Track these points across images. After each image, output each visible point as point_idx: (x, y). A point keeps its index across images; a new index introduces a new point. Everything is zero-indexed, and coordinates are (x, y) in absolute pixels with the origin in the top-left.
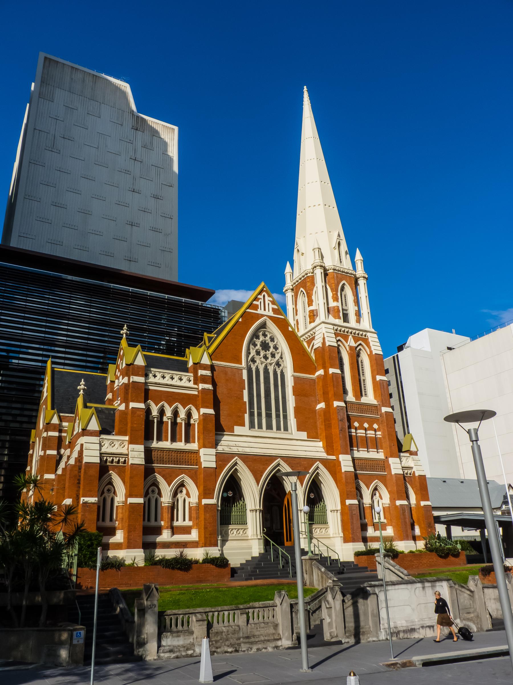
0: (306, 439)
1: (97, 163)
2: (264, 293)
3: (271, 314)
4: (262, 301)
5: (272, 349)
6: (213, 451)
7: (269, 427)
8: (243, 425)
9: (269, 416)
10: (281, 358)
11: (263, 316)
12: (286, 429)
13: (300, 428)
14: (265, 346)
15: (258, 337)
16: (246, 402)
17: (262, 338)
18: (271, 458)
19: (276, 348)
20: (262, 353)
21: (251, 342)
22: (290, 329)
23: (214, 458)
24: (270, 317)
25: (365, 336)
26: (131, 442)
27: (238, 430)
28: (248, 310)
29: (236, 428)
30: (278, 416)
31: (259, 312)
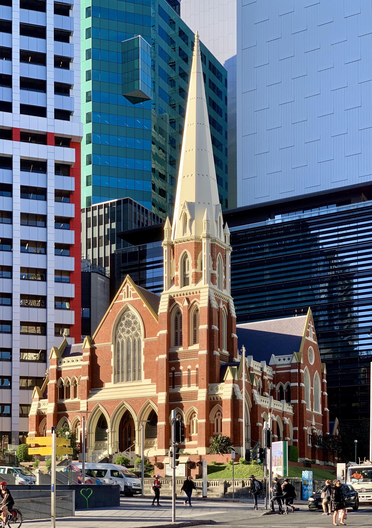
0: (151, 383)
3: (131, 299)
4: (126, 291)
6: (85, 401)
7: (128, 380)
9: (128, 372)
10: (140, 329)
11: (125, 302)
12: (139, 378)
13: (146, 378)
14: (128, 324)
16: (112, 366)
18: (118, 401)
19: (136, 323)
20: (127, 329)
21: (118, 324)
25: (200, 292)
28: (116, 302)
30: (134, 371)
31: (124, 300)
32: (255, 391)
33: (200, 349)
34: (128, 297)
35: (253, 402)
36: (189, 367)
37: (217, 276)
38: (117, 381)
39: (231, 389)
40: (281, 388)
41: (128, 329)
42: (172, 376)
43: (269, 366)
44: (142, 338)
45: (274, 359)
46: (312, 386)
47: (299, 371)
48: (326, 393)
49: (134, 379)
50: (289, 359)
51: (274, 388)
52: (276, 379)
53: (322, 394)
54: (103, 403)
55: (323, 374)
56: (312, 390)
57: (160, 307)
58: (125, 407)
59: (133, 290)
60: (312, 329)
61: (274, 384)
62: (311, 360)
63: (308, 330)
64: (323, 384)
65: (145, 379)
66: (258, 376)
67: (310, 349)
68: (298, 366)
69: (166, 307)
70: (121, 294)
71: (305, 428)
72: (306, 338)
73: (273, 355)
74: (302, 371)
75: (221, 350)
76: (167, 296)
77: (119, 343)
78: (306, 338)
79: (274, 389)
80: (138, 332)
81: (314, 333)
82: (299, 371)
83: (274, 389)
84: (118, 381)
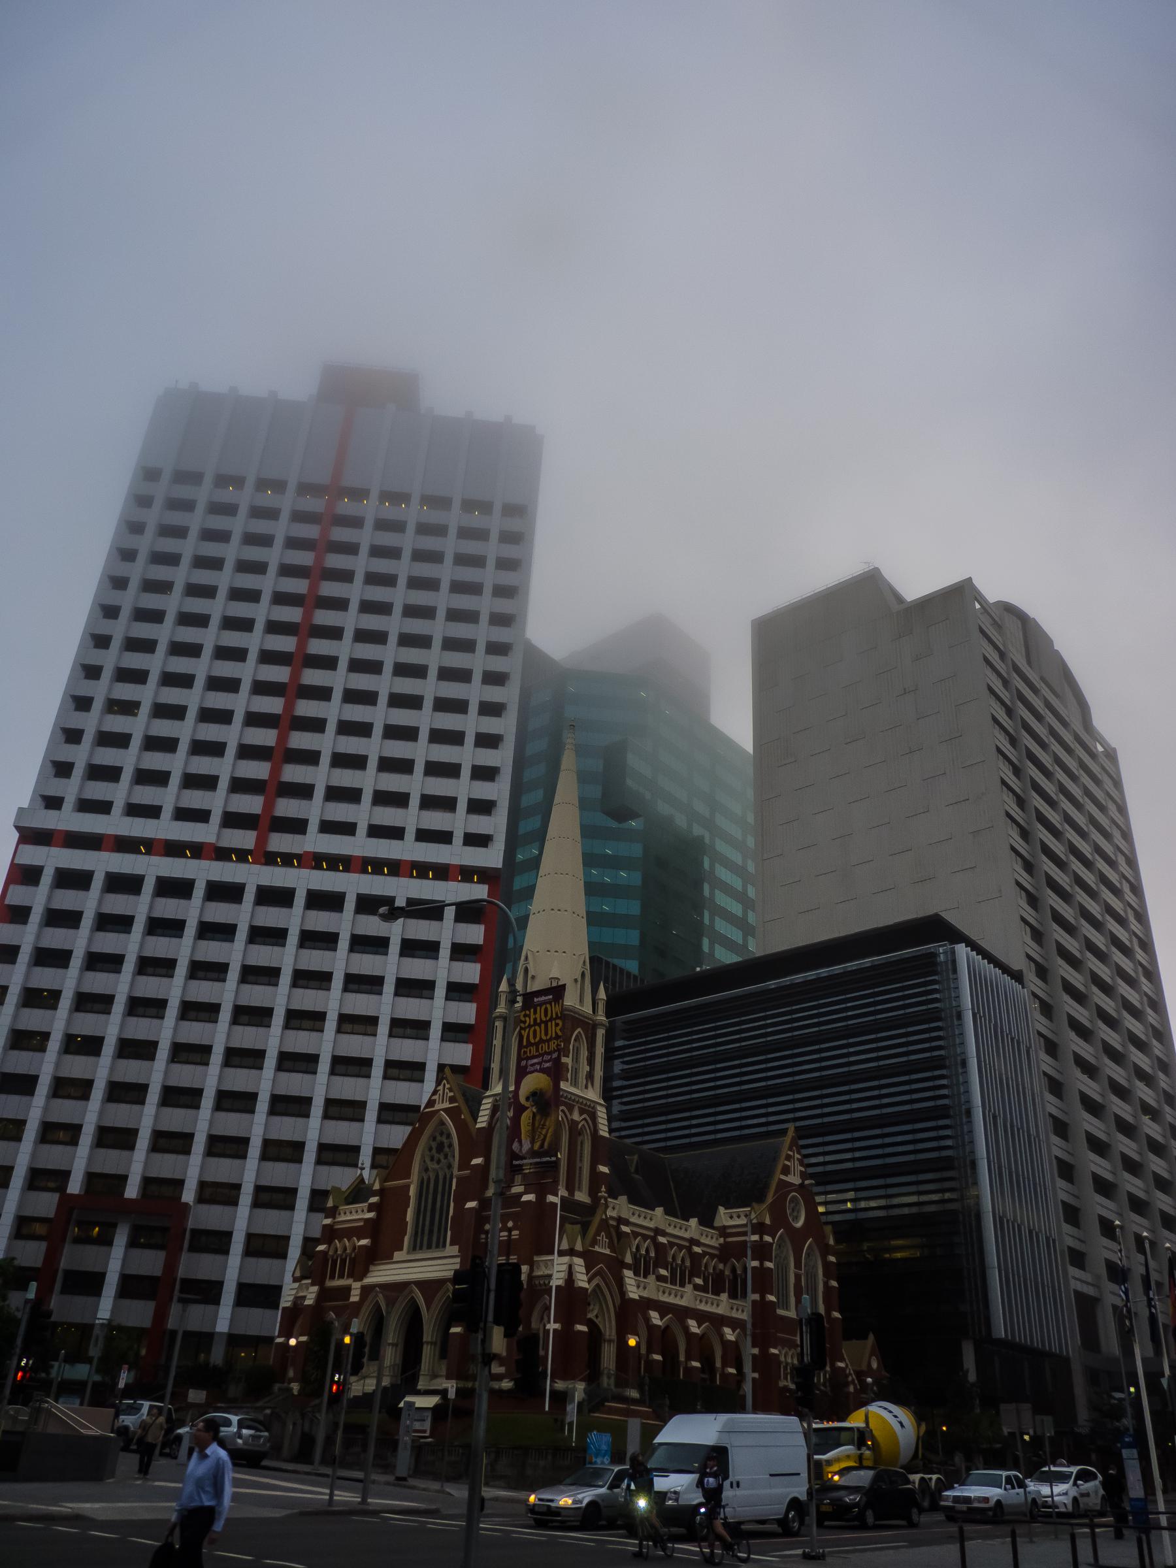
1: (849, 741)
2: (445, 1081)
3: (447, 1105)
4: (441, 1092)
5: (446, 1149)
7: (429, 1247)
8: (401, 1249)
9: (431, 1232)
10: (454, 1156)
11: (439, 1110)
12: (444, 1246)
13: (451, 1244)
14: (440, 1148)
15: (434, 1139)
17: (439, 1138)
19: (451, 1146)
22: (463, 1117)
23: (358, 1292)
24: (444, 1110)
26: (313, 1284)
27: (398, 1255)
29: (396, 1254)
31: (437, 1107)
32: (628, 1273)
33: (526, 1193)
34: (443, 1102)
35: (622, 1292)
36: (510, 1224)
37: (570, 1067)
38: (414, 1248)
39: (565, 1267)
40: (734, 1270)
41: (438, 1155)
42: (483, 1241)
43: (713, 1228)
44: (456, 1172)
45: (724, 1216)
46: (798, 1265)
47: (761, 1238)
48: (834, 1283)
49: (437, 1246)
50: (746, 1216)
51: (721, 1270)
52: (728, 1252)
53: (826, 1284)
54: (386, 1287)
55: (827, 1245)
56: (798, 1277)
57: (479, 1120)
58: (413, 1297)
59: (451, 1090)
60: (796, 1162)
61: (721, 1262)
62: (796, 1218)
63: (787, 1163)
64: (827, 1265)
65: (451, 1244)
66: (681, 1247)
67: (794, 1197)
68: (760, 1228)
69: (486, 1118)
70: (434, 1098)
71: (774, 1351)
72: (783, 1177)
73: (721, 1210)
74: (768, 1239)
75: (571, 1193)
76: (490, 1100)
77: (423, 1179)
78: (783, 1177)
79: (722, 1272)
80: (451, 1160)
81: (803, 1169)
82: (761, 1238)
83: (722, 1272)
84: (414, 1249)
